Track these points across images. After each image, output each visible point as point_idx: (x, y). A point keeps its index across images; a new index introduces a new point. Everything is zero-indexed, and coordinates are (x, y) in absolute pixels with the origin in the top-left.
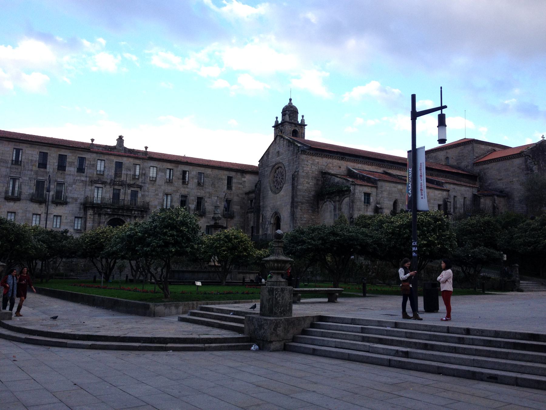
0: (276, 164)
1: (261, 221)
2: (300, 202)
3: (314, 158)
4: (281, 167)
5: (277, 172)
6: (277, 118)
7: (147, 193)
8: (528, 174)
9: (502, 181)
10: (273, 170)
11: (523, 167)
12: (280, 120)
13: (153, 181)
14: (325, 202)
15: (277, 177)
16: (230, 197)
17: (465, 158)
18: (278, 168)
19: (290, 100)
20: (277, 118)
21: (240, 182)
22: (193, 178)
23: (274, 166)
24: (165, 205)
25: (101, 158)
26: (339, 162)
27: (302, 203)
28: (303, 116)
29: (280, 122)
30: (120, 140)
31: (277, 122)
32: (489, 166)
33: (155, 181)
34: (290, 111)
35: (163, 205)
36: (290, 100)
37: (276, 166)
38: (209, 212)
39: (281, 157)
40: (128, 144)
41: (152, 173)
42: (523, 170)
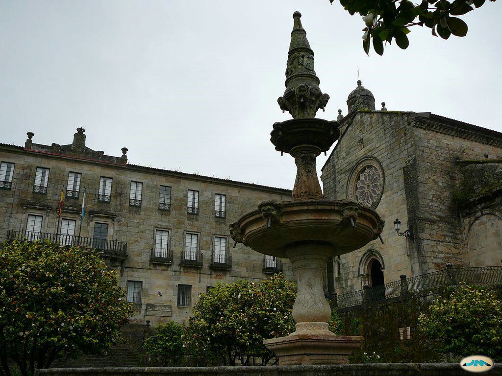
0: (358, 164)
1: (336, 275)
2: (427, 220)
3: (439, 136)
4: (369, 167)
5: (362, 177)
6: (340, 111)
7: (124, 229)
10: (354, 176)
12: (345, 113)
13: (136, 208)
14: (477, 218)
15: (362, 188)
18: (363, 171)
19: (359, 83)
20: (340, 111)
23: (352, 170)
24: (157, 250)
25: (42, 165)
26: (482, 146)
27: (432, 222)
28: (383, 104)
30: (80, 135)
33: (140, 207)
35: (153, 250)
36: (359, 83)
37: (360, 167)
38: (238, 264)
39: (368, 147)
40: (92, 143)
41: (134, 193)
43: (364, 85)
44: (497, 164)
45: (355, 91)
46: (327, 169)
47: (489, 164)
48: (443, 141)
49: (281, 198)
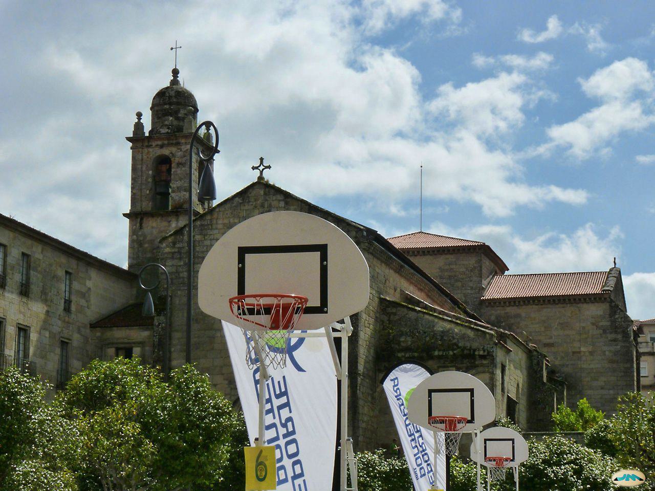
6: (139, 115)
8: (615, 340)
9: (553, 349)
11: (605, 323)
16: (66, 333)
17: (459, 284)
19: (175, 72)
20: (139, 115)
21: (84, 290)
22: (13, 268)
29: (147, 128)
31: (139, 126)
32: (523, 311)
34: (174, 104)
36: (175, 72)
42: (604, 331)
43: (186, 82)
44: (436, 320)
45: (167, 88)
46: (174, 243)
47: (427, 316)
48: (377, 270)
49: (78, 265)
